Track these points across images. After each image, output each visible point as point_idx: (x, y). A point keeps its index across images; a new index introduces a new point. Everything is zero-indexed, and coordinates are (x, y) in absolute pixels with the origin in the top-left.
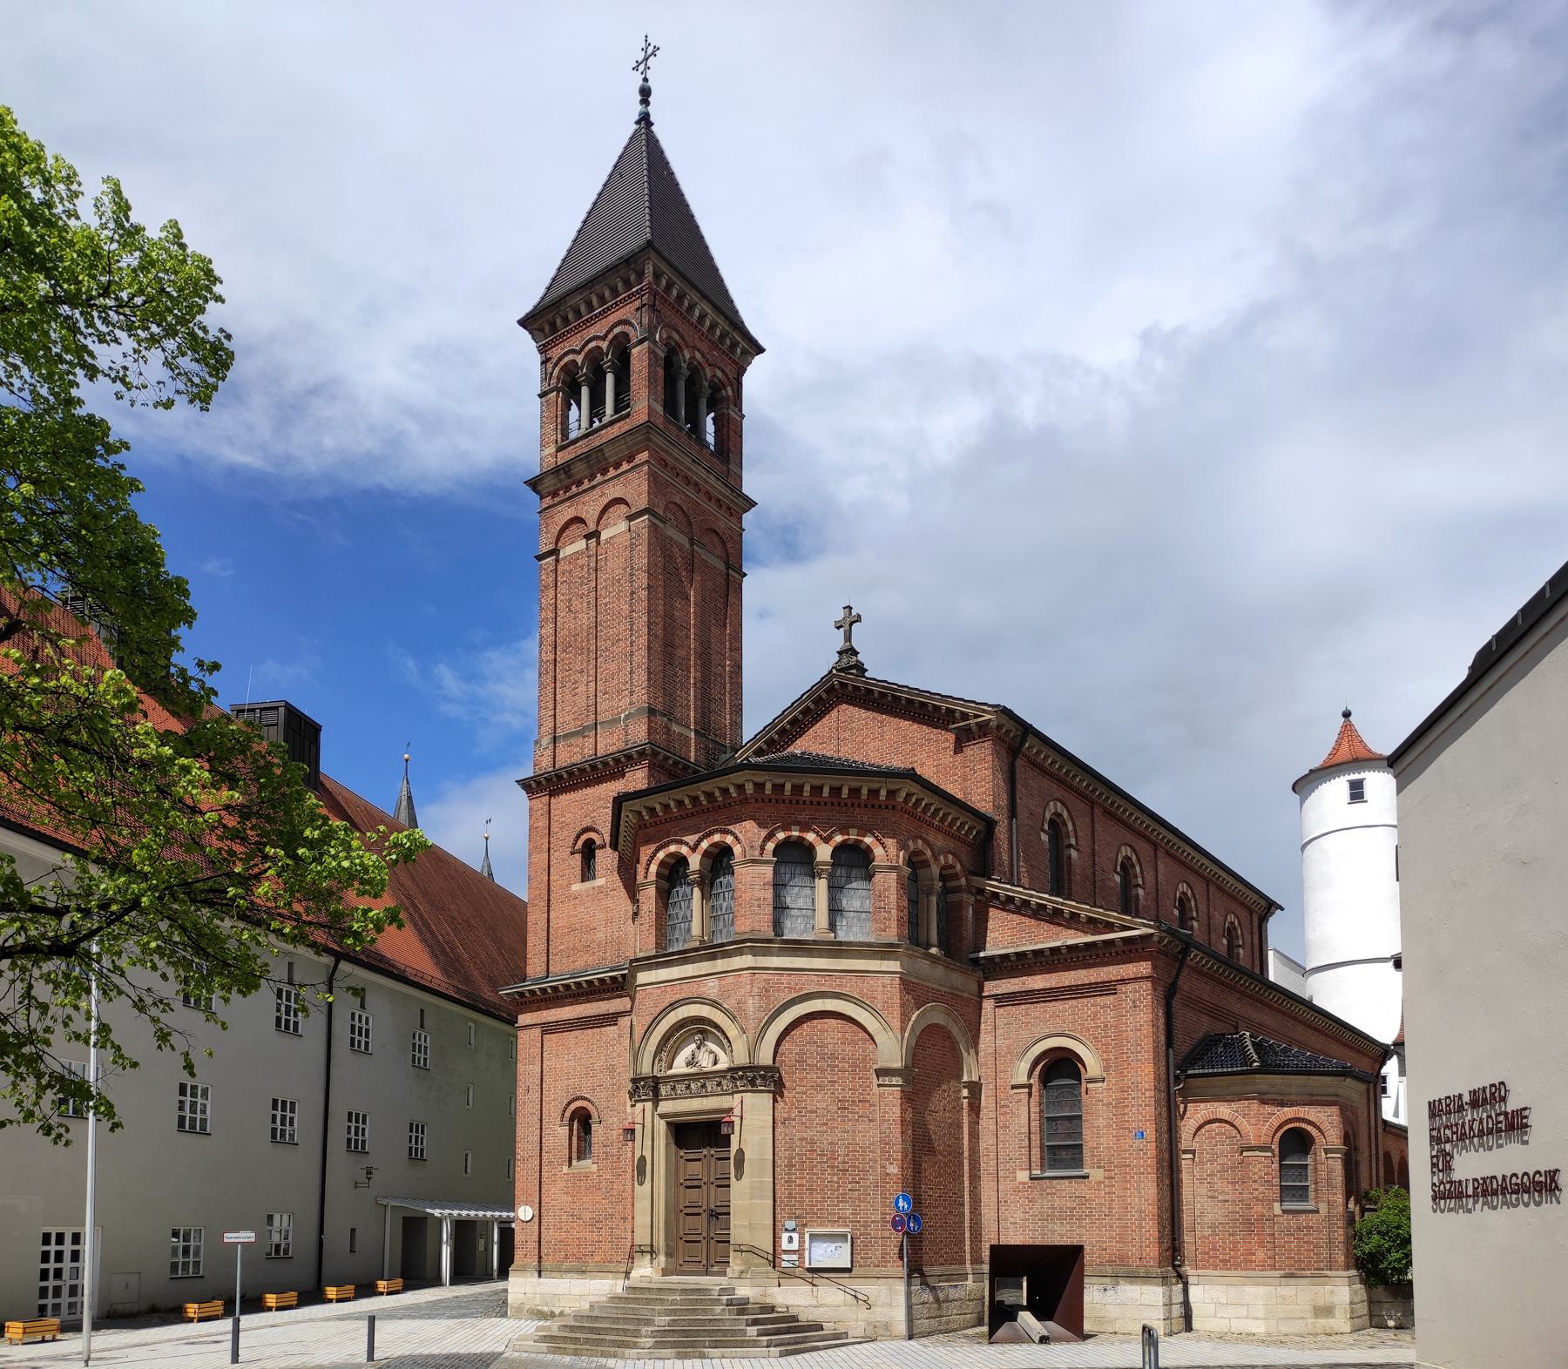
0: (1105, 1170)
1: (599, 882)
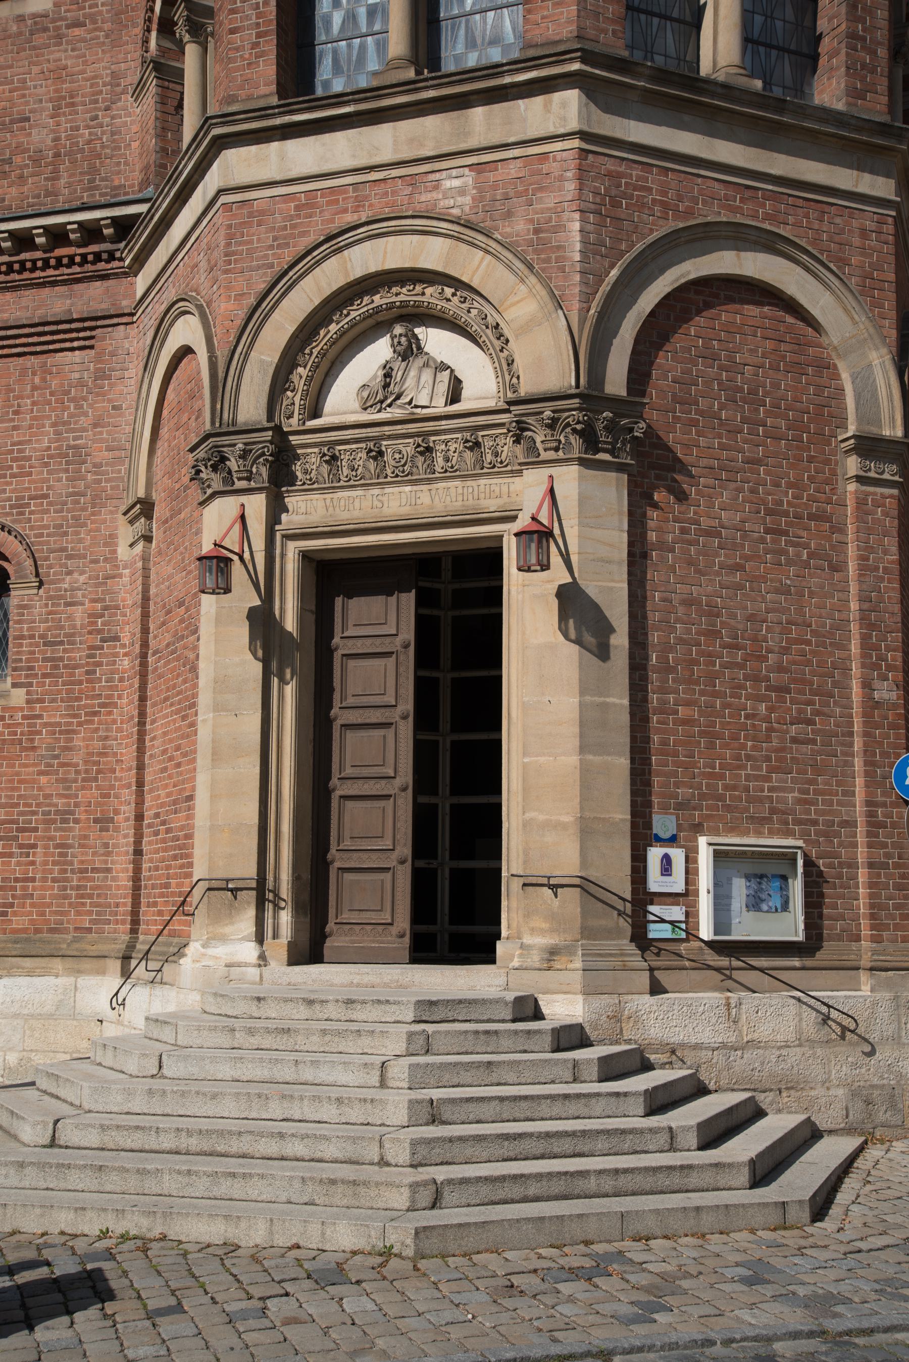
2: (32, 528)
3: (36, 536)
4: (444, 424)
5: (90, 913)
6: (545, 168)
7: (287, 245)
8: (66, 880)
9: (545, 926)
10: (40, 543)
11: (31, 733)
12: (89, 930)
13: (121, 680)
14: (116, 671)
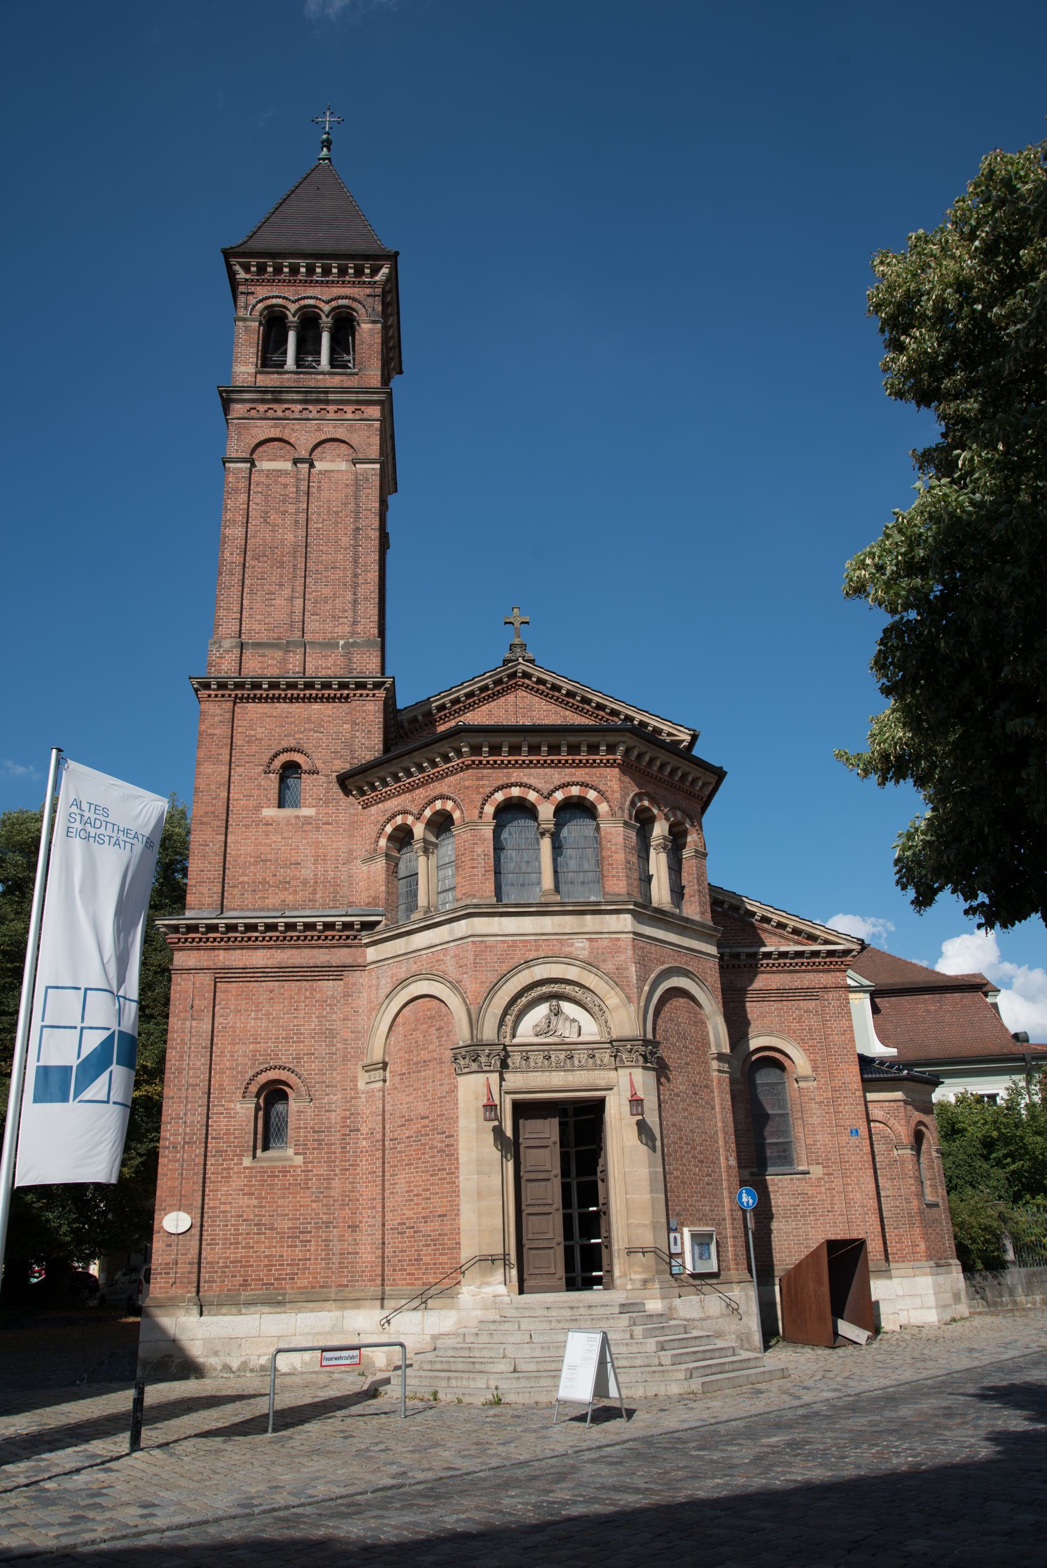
1: (307, 812)
5: (347, 1276)
6: (619, 943)
8: (330, 1259)
12: (347, 1286)
13: (362, 1152)
14: (358, 1147)
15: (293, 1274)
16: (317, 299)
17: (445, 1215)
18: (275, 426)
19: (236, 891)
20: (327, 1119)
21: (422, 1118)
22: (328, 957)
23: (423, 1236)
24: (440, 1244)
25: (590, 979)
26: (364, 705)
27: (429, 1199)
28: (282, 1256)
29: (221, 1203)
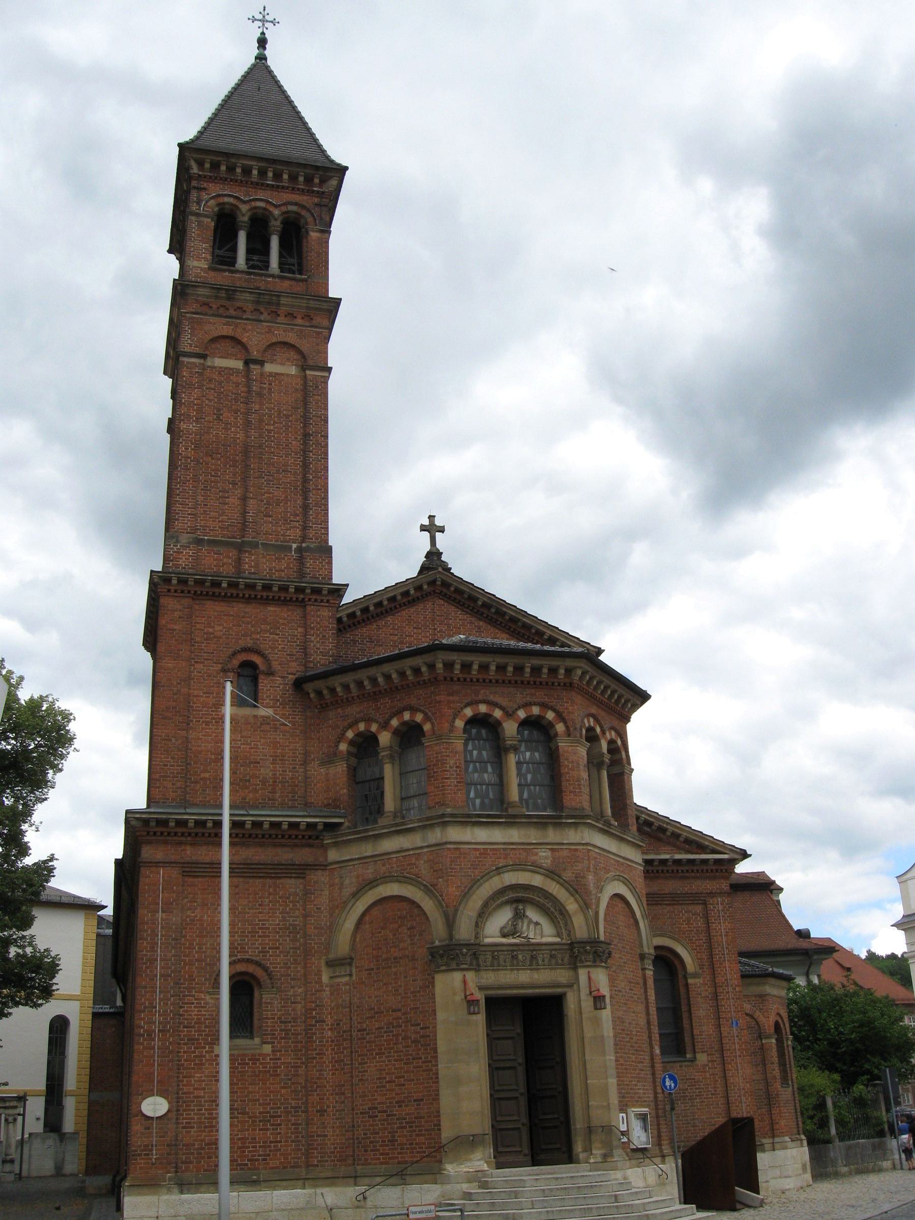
0: (708, 1055)
2: (271, 964)
3: (273, 968)
4: (544, 947)
6: (578, 854)
7: (476, 869)
8: (299, 1141)
9: (600, 1145)
10: (275, 971)
11: (275, 1067)
12: (317, 1166)
13: (327, 1041)
14: (324, 1037)
15: (265, 1155)
16: (267, 202)
17: (422, 1100)
18: (227, 324)
19: (198, 787)
20: (293, 1010)
21: (393, 1011)
22: (291, 856)
23: (397, 1119)
24: (416, 1126)
25: (554, 888)
26: (319, 610)
27: (404, 1085)
28: (255, 1139)
29: (195, 1089)
